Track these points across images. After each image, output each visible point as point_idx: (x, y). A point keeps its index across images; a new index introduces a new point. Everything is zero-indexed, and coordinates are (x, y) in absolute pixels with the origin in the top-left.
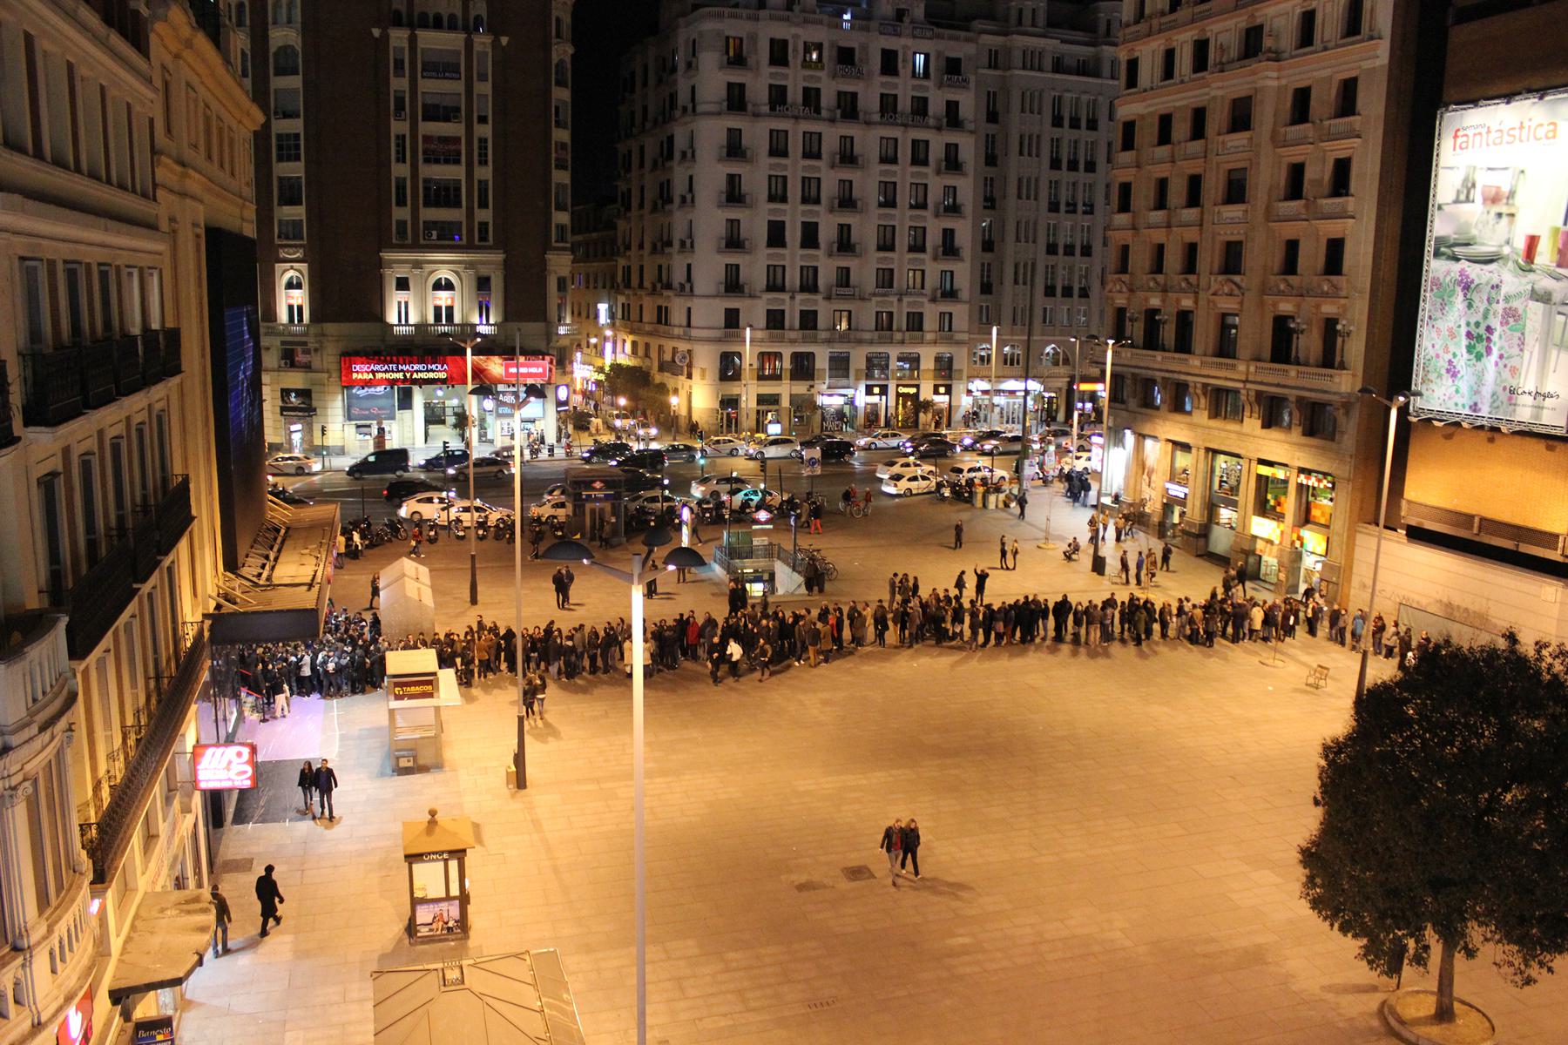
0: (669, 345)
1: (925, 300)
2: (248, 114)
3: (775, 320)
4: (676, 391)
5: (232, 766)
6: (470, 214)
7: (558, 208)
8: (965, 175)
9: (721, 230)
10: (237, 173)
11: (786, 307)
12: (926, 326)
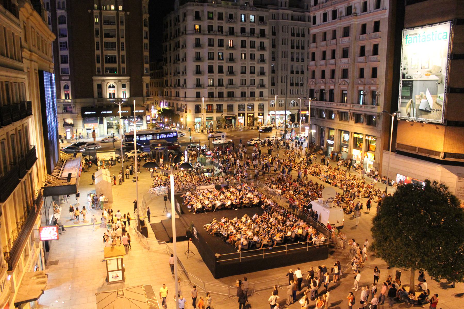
0: (180, 103)
1: (255, 88)
2: (51, 36)
3: (211, 95)
4: (182, 116)
5: (51, 233)
7: (145, 63)
8: (266, 51)
9: (195, 69)
10: (48, 54)
11: (214, 91)
12: (256, 95)
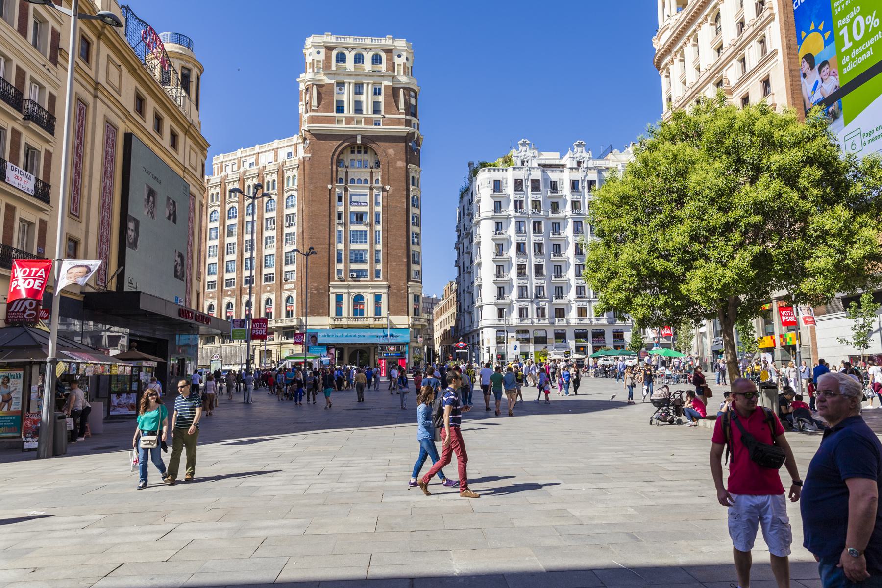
5: (27, 311)
6: (372, 266)
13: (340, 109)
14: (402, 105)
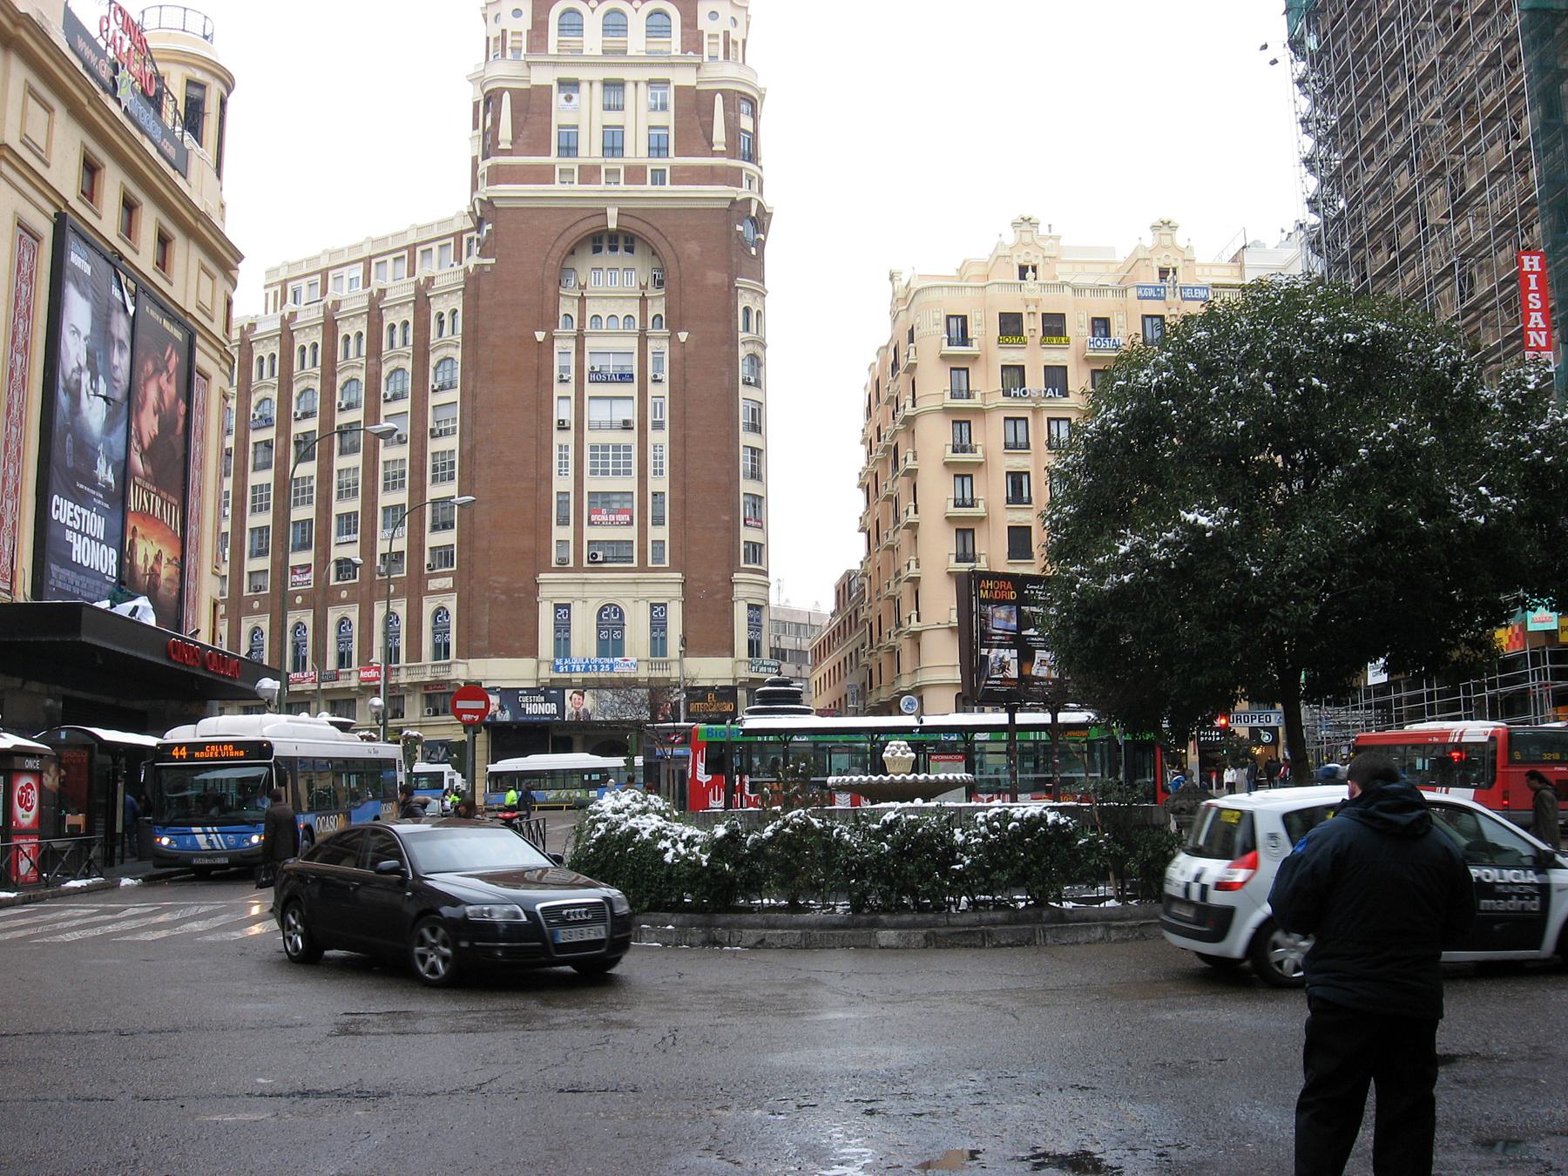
13: (569, 150)
14: (719, 134)
